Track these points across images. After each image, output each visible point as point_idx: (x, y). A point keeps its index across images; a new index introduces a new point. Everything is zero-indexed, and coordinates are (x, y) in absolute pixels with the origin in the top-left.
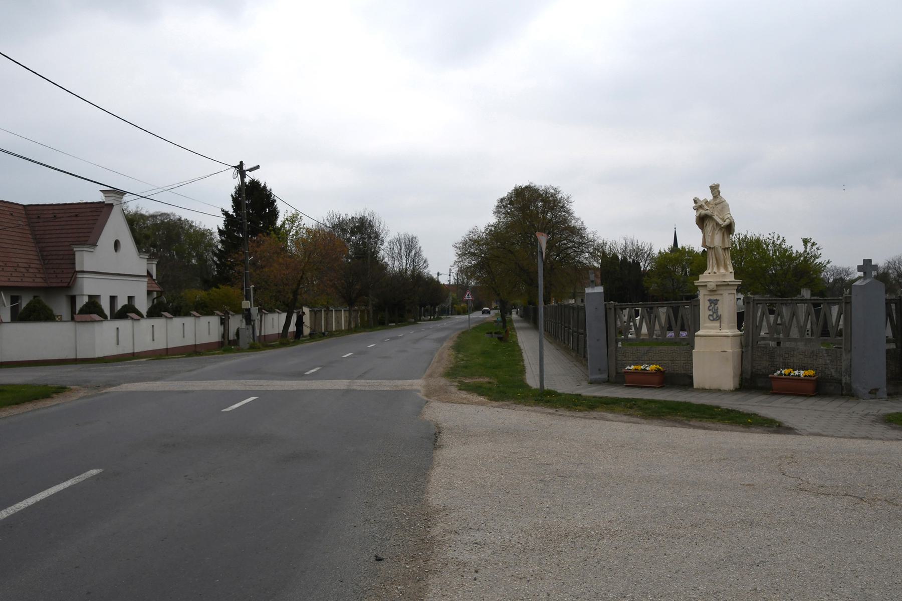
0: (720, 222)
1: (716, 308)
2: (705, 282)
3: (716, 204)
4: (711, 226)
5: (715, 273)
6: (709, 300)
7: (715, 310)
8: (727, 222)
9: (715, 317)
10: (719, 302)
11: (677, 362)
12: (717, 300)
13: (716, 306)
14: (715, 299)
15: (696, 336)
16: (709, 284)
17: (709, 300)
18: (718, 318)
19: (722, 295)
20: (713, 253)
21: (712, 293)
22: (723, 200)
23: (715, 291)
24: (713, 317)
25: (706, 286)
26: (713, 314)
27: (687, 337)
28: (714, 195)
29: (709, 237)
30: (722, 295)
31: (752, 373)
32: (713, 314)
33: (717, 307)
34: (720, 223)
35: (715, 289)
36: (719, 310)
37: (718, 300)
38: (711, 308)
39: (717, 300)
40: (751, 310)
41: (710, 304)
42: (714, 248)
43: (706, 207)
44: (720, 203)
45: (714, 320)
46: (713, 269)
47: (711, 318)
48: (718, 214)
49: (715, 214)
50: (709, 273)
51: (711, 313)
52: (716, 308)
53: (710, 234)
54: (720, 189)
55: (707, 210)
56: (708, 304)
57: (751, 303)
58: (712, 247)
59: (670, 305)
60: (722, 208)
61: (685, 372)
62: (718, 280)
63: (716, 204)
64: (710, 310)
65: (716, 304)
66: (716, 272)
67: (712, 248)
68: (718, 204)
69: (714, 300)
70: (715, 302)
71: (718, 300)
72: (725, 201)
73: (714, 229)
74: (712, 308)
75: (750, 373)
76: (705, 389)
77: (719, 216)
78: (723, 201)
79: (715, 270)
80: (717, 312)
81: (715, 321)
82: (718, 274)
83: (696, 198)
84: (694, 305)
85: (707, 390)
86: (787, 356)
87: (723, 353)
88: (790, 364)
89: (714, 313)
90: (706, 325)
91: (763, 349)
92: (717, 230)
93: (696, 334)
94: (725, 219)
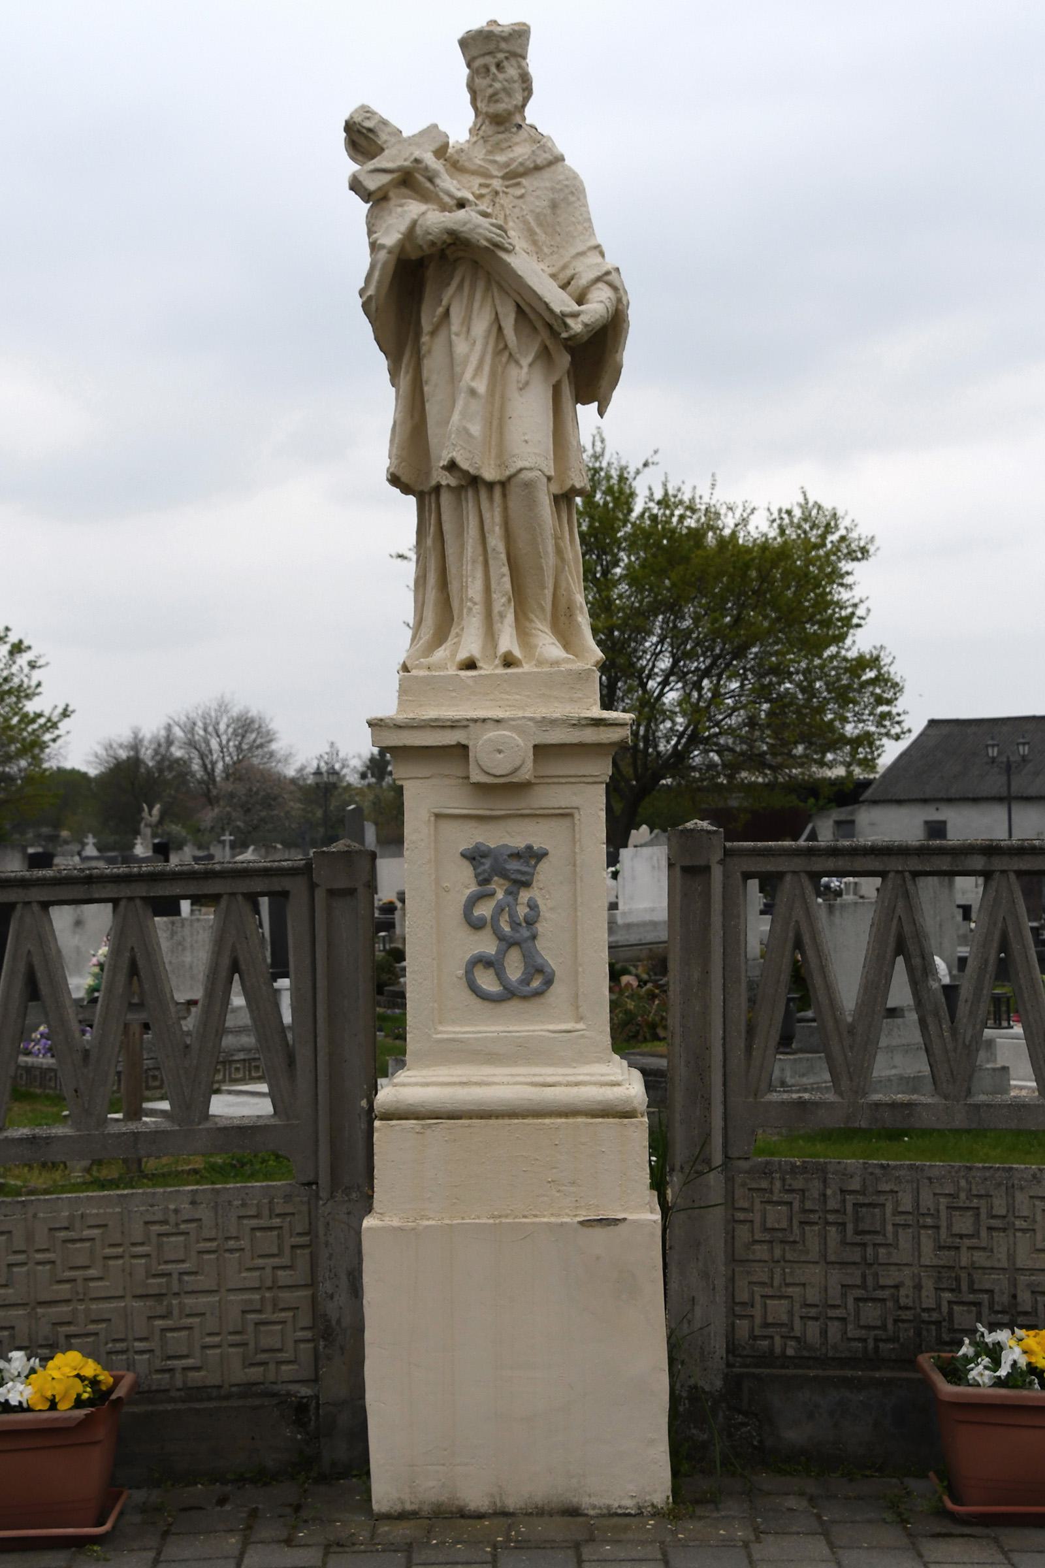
0: (559, 301)
1: (522, 911)
2: (454, 725)
3: (513, 175)
4: (481, 325)
5: (509, 662)
6: (474, 857)
7: (514, 924)
8: (597, 306)
9: (514, 970)
10: (543, 866)
11: (189, 1301)
12: (534, 856)
13: (524, 896)
14: (518, 842)
15: (387, 1116)
16: (481, 743)
17: (474, 857)
18: (536, 984)
19: (566, 815)
20: (493, 518)
21: (501, 807)
23: (525, 786)
24: (500, 976)
25: (462, 750)
26: (502, 953)
27: (273, 1121)
28: (494, 108)
29: (475, 406)
30: (566, 815)
31: (732, 1348)
32: (502, 953)
33: (533, 906)
34: (557, 309)
35: (526, 773)
36: (540, 927)
37: (540, 856)
38: (484, 910)
39: (534, 856)
40: (717, 920)
41: (484, 881)
42: (504, 484)
43: (449, 184)
44: (538, 168)
45: (509, 994)
46: (490, 635)
47: (487, 981)
49: (516, 237)
50: (471, 665)
51: (488, 945)
52: (522, 911)
53: (481, 387)
54: (537, 61)
55: (461, 204)
56: (463, 879)
57: (717, 872)
58: (489, 474)
59: (141, 890)
60: (554, 206)
61: (255, 1373)
62: (557, 711)
63: (513, 175)
64: (476, 925)
65: (527, 885)
66: (517, 653)
67: (490, 486)
68: (527, 173)
69: (517, 855)
70: (514, 865)
71: (540, 856)
72: (560, 159)
73: (502, 348)
74: (499, 910)
75: (719, 1346)
76: (463, 1514)
79: (507, 642)
80: (534, 937)
81: (513, 1006)
83: (367, 111)
84: (332, 893)
85: (480, 1516)
86: (963, 1224)
87: (599, 1233)
88: (986, 1281)
89: (507, 943)
90: (449, 1031)
91: (798, 1184)
92: (525, 362)
93: (387, 1093)
94: (584, 280)
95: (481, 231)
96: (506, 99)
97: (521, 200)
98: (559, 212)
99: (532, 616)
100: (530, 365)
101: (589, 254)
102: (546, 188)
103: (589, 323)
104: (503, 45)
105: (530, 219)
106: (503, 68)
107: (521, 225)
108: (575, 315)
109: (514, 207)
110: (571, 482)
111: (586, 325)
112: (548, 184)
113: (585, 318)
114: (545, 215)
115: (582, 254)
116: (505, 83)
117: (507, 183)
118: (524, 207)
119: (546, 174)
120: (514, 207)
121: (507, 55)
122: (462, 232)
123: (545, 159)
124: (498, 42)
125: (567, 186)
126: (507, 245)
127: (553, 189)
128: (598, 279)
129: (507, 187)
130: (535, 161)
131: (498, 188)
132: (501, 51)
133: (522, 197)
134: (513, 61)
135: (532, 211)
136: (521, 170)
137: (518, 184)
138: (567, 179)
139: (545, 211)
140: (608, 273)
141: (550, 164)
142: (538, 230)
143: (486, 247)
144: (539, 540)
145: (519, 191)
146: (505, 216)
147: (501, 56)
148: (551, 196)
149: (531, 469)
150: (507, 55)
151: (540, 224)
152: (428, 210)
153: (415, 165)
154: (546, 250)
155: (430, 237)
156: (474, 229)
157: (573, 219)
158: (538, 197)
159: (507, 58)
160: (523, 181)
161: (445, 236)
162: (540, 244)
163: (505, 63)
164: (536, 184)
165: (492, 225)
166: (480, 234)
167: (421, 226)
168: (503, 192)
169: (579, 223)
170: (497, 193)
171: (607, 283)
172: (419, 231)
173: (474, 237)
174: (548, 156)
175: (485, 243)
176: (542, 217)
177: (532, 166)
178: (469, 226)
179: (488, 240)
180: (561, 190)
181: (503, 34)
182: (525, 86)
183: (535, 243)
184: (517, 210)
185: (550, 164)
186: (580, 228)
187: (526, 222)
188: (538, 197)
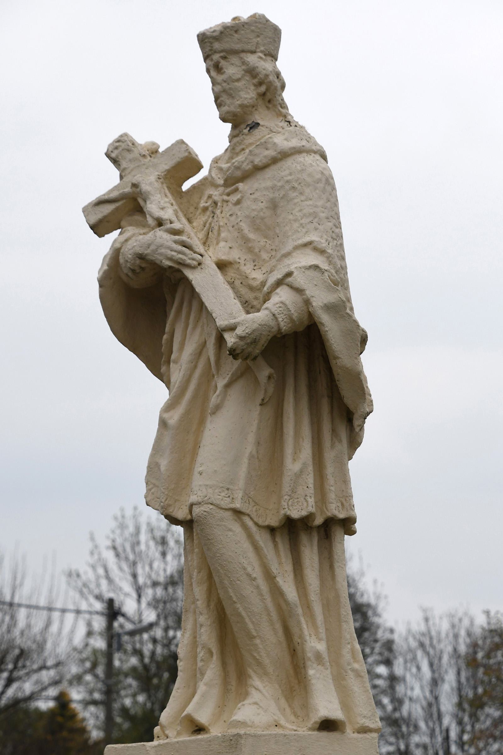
22: (294, 143)
44: (258, 169)
48: (235, 255)
55: (160, 223)
60: (274, 206)
68: (245, 176)
77: (248, 269)
78: (284, 155)
82: (215, 731)
92: (221, 383)
95: (163, 251)
96: (228, 102)
97: (239, 206)
98: (279, 212)
99: (250, 672)
100: (228, 386)
101: (294, 254)
102: (266, 189)
103: (243, 335)
104: (217, 46)
105: (244, 226)
106: (222, 69)
107: (236, 234)
108: (232, 328)
109: (231, 215)
110: (283, 512)
111: (241, 338)
112: (269, 184)
113: (239, 331)
114: (263, 219)
115: (288, 255)
116: (224, 84)
117: (229, 190)
118: (239, 214)
119: (269, 173)
120: (231, 215)
121: (222, 54)
122: (146, 255)
123: (265, 157)
124: (211, 43)
125: (288, 181)
126: (189, 261)
127: (273, 188)
128: (279, 283)
129: (228, 195)
130: (252, 162)
131: (216, 198)
132: (215, 52)
133: (238, 202)
134: (234, 59)
135: (247, 217)
136: (238, 173)
137: (237, 190)
138: (290, 174)
139: (262, 214)
140: (289, 274)
141: (275, 161)
142: (251, 236)
143: (170, 267)
144: (226, 582)
145: (234, 198)
146: (219, 227)
147: (216, 57)
148: (271, 195)
149: (199, 503)
150: (222, 54)
151: (257, 229)
152: (134, 235)
153: (134, 189)
154: (265, 256)
155: (128, 265)
156: (156, 250)
157: (291, 217)
158: (255, 200)
159: (224, 58)
160: (240, 185)
161: (138, 261)
162: (257, 250)
163: (223, 63)
164: (256, 185)
165: (176, 242)
166: (161, 254)
167: (122, 253)
168: (223, 201)
169: (295, 220)
170: (216, 203)
171: (291, 287)
172: (121, 261)
173: (157, 258)
174: (271, 153)
175: (168, 263)
176: (258, 221)
177: (250, 166)
178: (153, 247)
179: (171, 259)
180: (282, 187)
181: (215, 34)
182: (255, 81)
183: (250, 250)
184: (234, 217)
185: (275, 161)
186: (296, 225)
187: (240, 230)
188: (255, 200)
